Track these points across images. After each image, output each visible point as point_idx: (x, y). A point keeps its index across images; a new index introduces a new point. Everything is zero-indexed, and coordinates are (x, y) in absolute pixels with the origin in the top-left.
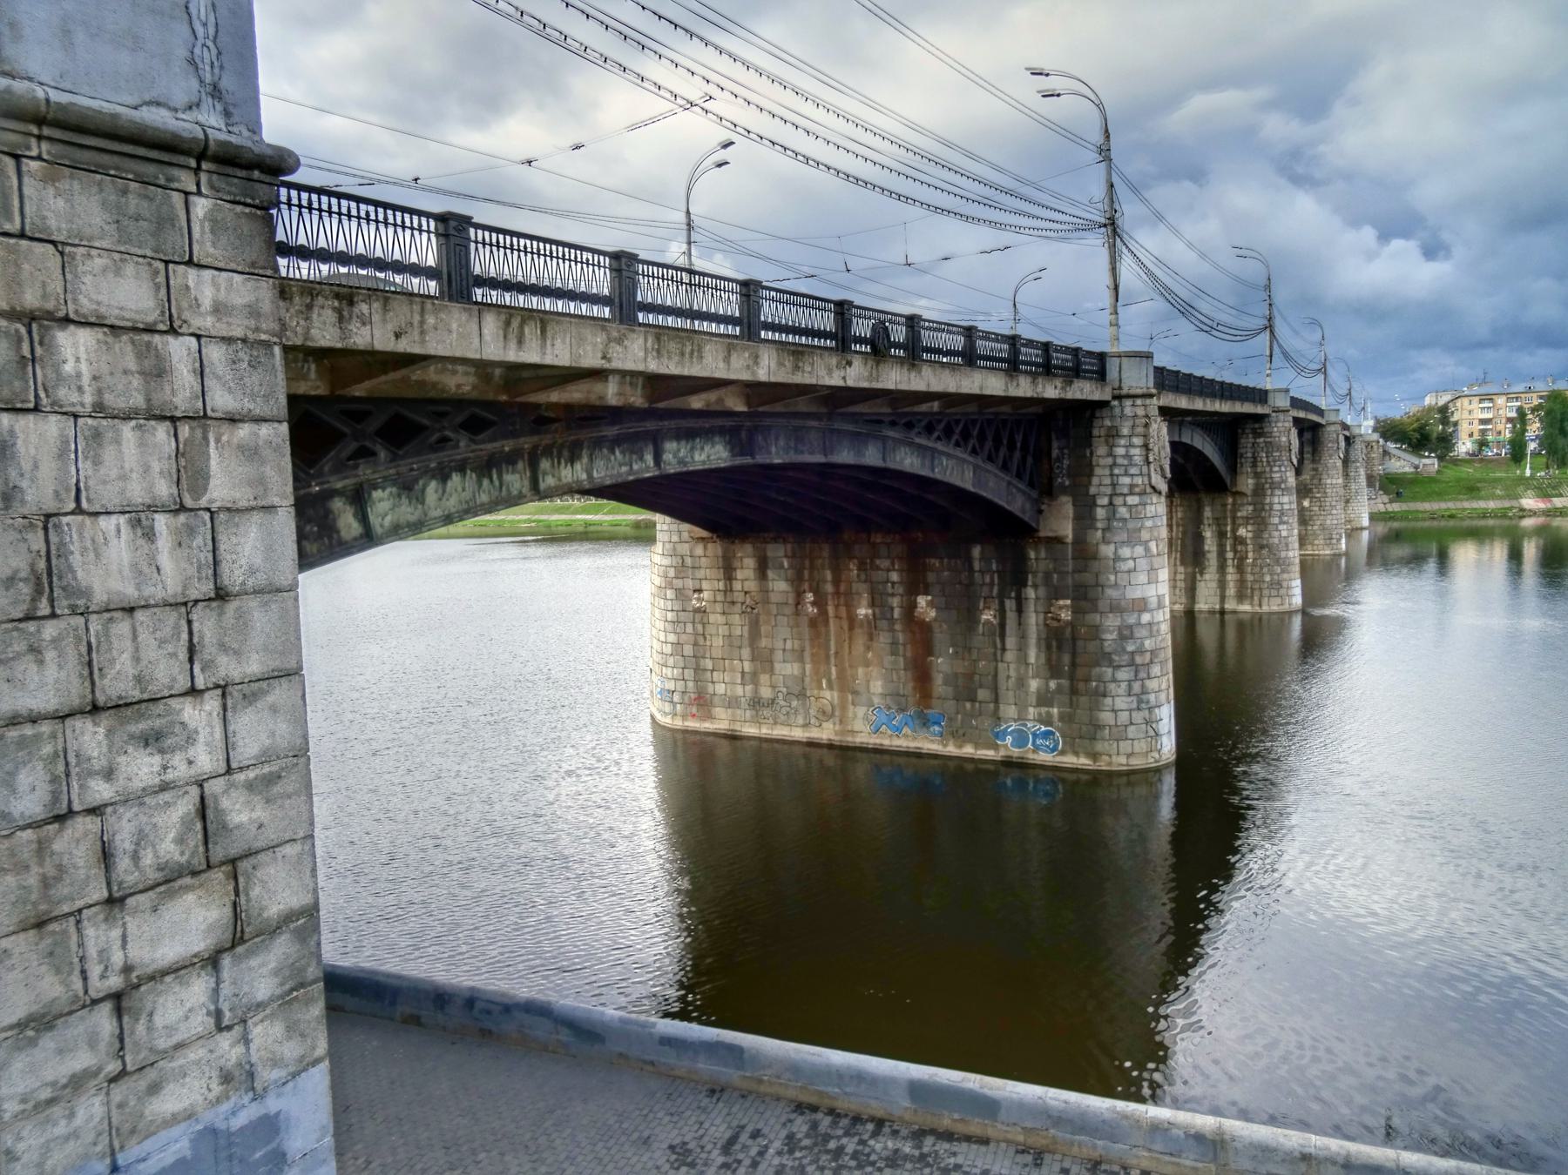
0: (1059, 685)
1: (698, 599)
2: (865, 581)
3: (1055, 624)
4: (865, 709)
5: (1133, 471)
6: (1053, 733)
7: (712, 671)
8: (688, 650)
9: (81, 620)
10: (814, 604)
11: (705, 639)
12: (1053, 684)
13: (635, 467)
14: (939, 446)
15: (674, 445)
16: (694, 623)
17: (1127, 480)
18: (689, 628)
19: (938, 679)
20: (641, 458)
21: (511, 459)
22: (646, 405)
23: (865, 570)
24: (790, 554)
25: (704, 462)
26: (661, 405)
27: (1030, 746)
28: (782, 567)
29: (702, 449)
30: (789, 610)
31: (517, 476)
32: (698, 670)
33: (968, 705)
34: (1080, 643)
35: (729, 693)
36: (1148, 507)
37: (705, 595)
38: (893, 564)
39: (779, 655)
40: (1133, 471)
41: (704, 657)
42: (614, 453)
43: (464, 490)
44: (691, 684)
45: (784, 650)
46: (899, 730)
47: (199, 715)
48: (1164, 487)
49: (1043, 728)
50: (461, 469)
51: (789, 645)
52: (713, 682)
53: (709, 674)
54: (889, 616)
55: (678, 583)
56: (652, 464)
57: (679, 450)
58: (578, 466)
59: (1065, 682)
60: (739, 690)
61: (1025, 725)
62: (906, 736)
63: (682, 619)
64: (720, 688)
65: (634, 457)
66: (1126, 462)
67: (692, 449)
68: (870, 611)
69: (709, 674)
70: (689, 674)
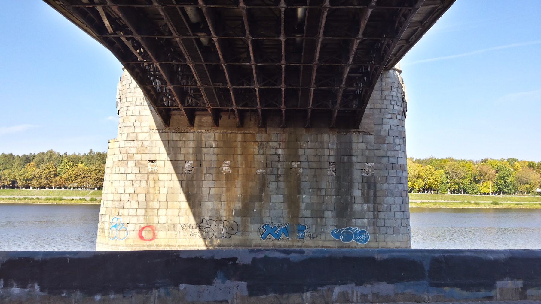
0: (368, 208)
3: (366, 175)
4: (258, 226)
6: (365, 232)
8: (142, 197)
11: (155, 190)
12: (365, 206)
19: (303, 206)
23: (263, 148)
27: (353, 240)
28: (211, 147)
30: (213, 171)
33: (319, 220)
34: (378, 185)
35: (169, 222)
38: (279, 144)
39: (205, 198)
44: (142, 219)
46: (278, 236)
49: (360, 230)
51: (213, 191)
53: (156, 211)
59: (371, 205)
60: (176, 220)
61: (350, 229)
62: (283, 239)
66: (396, 99)
68: (264, 171)
69: (156, 211)
70: (141, 212)
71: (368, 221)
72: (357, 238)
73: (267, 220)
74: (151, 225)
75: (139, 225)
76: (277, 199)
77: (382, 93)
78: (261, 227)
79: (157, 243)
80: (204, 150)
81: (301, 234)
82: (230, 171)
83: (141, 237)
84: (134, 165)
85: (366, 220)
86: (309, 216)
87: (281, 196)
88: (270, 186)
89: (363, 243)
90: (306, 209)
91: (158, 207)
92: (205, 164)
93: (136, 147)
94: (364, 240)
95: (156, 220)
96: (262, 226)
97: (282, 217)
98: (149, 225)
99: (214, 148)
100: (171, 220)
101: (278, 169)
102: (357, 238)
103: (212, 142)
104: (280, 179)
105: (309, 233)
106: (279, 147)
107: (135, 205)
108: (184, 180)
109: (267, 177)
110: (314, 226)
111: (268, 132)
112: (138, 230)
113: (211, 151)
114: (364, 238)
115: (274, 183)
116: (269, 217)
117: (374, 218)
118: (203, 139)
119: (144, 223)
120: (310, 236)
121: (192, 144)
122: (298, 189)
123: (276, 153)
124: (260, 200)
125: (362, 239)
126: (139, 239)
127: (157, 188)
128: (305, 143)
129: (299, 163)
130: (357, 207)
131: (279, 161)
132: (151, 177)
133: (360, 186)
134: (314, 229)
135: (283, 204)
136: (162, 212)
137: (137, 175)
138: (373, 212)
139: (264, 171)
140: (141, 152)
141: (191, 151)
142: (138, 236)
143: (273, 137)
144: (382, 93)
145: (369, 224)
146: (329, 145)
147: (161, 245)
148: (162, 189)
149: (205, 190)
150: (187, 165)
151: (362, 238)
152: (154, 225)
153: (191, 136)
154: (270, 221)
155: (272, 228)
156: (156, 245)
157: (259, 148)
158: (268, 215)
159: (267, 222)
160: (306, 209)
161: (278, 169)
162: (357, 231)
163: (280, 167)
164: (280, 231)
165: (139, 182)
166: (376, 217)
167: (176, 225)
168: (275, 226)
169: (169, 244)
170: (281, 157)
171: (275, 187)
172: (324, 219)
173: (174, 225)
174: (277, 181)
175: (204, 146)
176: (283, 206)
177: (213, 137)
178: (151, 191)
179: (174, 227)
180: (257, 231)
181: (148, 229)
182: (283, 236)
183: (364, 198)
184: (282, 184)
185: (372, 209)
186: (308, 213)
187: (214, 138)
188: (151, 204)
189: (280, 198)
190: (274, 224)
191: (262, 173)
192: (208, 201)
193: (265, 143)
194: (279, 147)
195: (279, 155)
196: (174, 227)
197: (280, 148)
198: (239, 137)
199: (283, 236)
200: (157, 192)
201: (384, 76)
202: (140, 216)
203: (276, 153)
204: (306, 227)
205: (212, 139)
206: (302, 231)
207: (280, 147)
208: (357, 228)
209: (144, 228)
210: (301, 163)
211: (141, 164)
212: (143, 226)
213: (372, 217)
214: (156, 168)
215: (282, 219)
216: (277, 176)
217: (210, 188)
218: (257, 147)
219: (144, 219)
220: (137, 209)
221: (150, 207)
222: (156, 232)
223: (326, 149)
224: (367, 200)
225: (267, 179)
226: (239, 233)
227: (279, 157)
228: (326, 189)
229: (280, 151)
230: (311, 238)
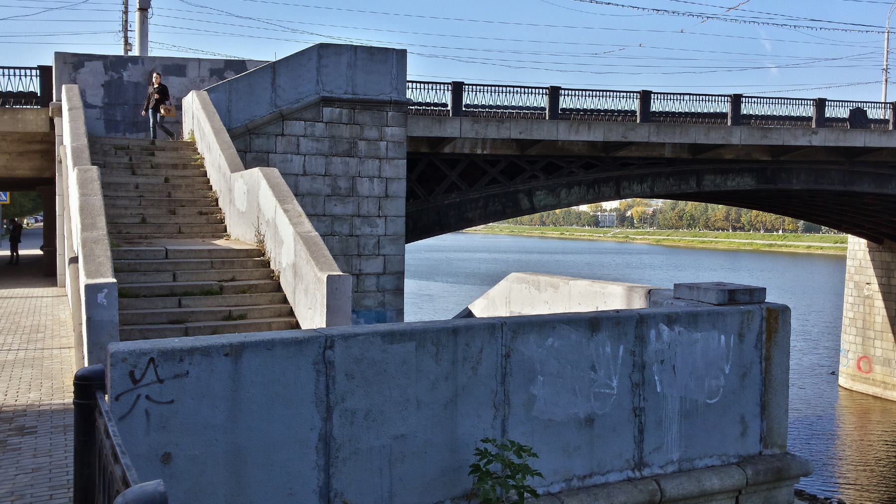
1: (868, 289)
7: (875, 339)
8: (860, 324)
9: (358, 198)
11: (871, 316)
13: (683, 187)
15: (712, 177)
16: (864, 305)
18: (861, 309)
21: (606, 181)
25: (735, 186)
29: (734, 179)
31: (609, 189)
32: (865, 338)
35: (884, 356)
42: (669, 180)
43: (580, 193)
44: (860, 347)
47: (380, 222)
50: (579, 184)
53: (872, 341)
56: (695, 186)
58: (645, 185)
63: (857, 302)
64: (879, 352)
67: (726, 179)
69: (872, 341)
70: (859, 340)
74: (868, 356)
75: (857, 354)
79: (874, 378)
83: (859, 368)
84: (853, 287)
91: (874, 338)
93: (855, 267)
95: (872, 353)
98: (867, 355)
100: (886, 354)
107: (854, 331)
112: (857, 359)
119: (862, 353)
126: (858, 369)
127: (873, 316)
132: (868, 301)
136: (878, 343)
140: (860, 273)
142: (857, 367)
147: (877, 381)
148: (877, 317)
152: (871, 356)
156: (872, 379)
165: (857, 306)
167: (891, 361)
169: (884, 381)
173: (889, 360)
178: (868, 317)
179: (889, 363)
181: (865, 360)
188: (868, 332)
196: (889, 363)
200: (872, 320)
209: (861, 358)
211: (859, 286)
212: (861, 355)
214: (871, 292)
221: (867, 336)
222: (873, 365)
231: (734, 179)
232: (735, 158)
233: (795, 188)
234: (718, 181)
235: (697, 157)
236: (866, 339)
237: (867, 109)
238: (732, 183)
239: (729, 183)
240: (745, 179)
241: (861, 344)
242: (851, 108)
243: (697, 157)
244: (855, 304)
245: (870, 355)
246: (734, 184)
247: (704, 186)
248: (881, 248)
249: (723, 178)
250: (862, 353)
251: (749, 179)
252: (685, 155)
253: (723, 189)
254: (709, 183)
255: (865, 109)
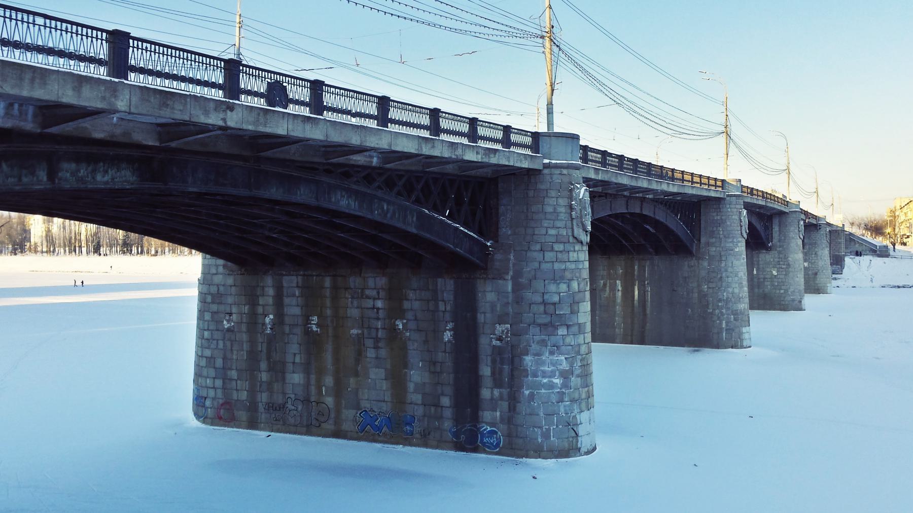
0: (501, 393)
2: (357, 308)
4: (355, 411)
5: (559, 224)
6: (496, 433)
8: (219, 363)
10: (318, 325)
12: (496, 392)
14: (379, 193)
15: (73, 166)
16: (223, 340)
17: (552, 232)
18: (221, 344)
19: (411, 387)
20: (33, 174)
22: (39, 131)
23: (357, 298)
24: (300, 285)
25: (107, 183)
26: (54, 130)
28: (294, 295)
33: (433, 409)
36: (571, 254)
37: (234, 317)
38: (378, 293)
39: (290, 367)
40: (559, 224)
41: (231, 369)
44: (219, 392)
45: (294, 363)
48: (586, 239)
52: (237, 390)
53: (234, 383)
54: (374, 335)
55: (214, 307)
56: (45, 179)
57: (79, 171)
59: (505, 392)
63: (215, 337)
65: (24, 172)
67: (94, 171)
69: (234, 383)
70: (219, 383)
71: (501, 415)
72: (485, 441)
73: (365, 405)
76: (377, 375)
77: (527, 209)
78: (358, 415)
80: (287, 301)
81: (408, 428)
82: (319, 330)
85: (498, 414)
86: (420, 402)
87: (383, 370)
88: (369, 355)
89: (493, 449)
90: (416, 391)
92: (287, 320)
94: (494, 444)
96: (359, 413)
97: (384, 401)
98: (228, 401)
99: (298, 297)
101: (377, 329)
102: (485, 441)
103: (295, 289)
104: (380, 345)
105: (419, 427)
106: (377, 297)
108: (264, 342)
109: (364, 341)
110: (426, 418)
111: (362, 275)
113: (294, 302)
114: (494, 441)
115: (373, 351)
116: (368, 400)
117: (510, 411)
118: (285, 284)
119: (222, 399)
120: (421, 433)
121: (271, 291)
122: (404, 364)
123: (374, 305)
124: (356, 374)
125: (492, 444)
128: (412, 291)
129: (405, 321)
130: (485, 393)
131: (378, 319)
133: (489, 358)
134: (426, 423)
135: (384, 381)
137: (213, 332)
138: (507, 403)
139: (360, 332)
141: (270, 301)
143: (371, 282)
144: (527, 209)
145: (502, 420)
146: (445, 295)
149: (289, 358)
150: (267, 320)
151: (492, 441)
152: (233, 401)
153: (269, 281)
154: (368, 406)
155: (371, 417)
157: (353, 298)
158: (366, 397)
159: (365, 408)
160: (416, 391)
161: (377, 329)
162: (485, 430)
163: (379, 327)
164: (382, 421)
166: (512, 409)
168: (374, 413)
170: (381, 311)
171: (374, 356)
172: (439, 409)
174: (376, 348)
175: (285, 294)
176: (385, 385)
177: (295, 281)
180: (353, 420)
182: (385, 429)
183: (494, 380)
184: (383, 353)
185: (506, 397)
186: (417, 398)
187: (297, 283)
188: (229, 372)
189: (381, 373)
190: (374, 411)
191: (358, 334)
192: (294, 372)
193: (360, 291)
194: (377, 297)
195: (378, 309)
197: (379, 299)
198: (328, 282)
199: (385, 429)
201: (533, 181)
202: (218, 388)
203: (374, 305)
204: (415, 418)
205: (294, 285)
206: (409, 424)
207: (379, 296)
208: (485, 425)
210: (407, 322)
213: (507, 410)
215: (384, 404)
216: (377, 340)
217: (295, 354)
218: (350, 297)
219: (222, 392)
220: (214, 378)
221: (229, 378)
223: (440, 301)
224: (498, 383)
225: (364, 345)
226: (331, 422)
227: (378, 313)
228: (441, 363)
229: (379, 304)
230: (421, 436)
231: (106, 172)
232: (109, 139)
233: (191, 189)
234: (82, 173)
235: (46, 131)
236: (227, 381)
237: (287, 84)
238: (103, 177)
239: (99, 177)
240: (123, 172)
241: (221, 387)
242: (269, 81)
243: (46, 131)
244: (214, 340)
245: (233, 400)
246: (106, 179)
247: (60, 179)
248: (243, 270)
249: (90, 169)
250: (222, 399)
251: (128, 173)
252: (29, 125)
253: (90, 186)
254: (68, 175)
255: (284, 84)
